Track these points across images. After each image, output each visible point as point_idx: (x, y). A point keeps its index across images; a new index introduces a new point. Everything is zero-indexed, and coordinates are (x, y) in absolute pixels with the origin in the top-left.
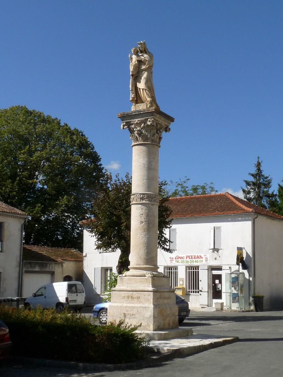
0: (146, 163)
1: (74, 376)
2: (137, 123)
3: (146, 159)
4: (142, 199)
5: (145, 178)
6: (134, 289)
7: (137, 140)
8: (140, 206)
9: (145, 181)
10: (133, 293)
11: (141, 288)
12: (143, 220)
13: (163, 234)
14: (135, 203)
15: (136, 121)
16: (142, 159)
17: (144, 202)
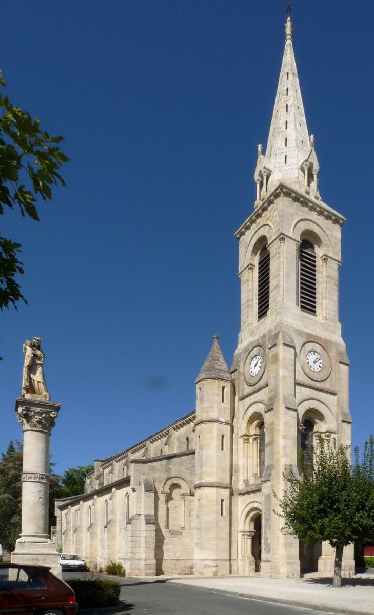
0: (44, 448)
1: (118, 614)
2: (39, 412)
3: (44, 445)
4: (41, 478)
5: (44, 461)
6: (38, 553)
7: (36, 426)
8: (39, 484)
9: (44, 463)
10: (38, 557)
11: (47, 552)
12: (42, 496)
13: (326, 546)
14: (33, 480)
15: (38, 410)
16: (41, 444)
17: (43, 481)
